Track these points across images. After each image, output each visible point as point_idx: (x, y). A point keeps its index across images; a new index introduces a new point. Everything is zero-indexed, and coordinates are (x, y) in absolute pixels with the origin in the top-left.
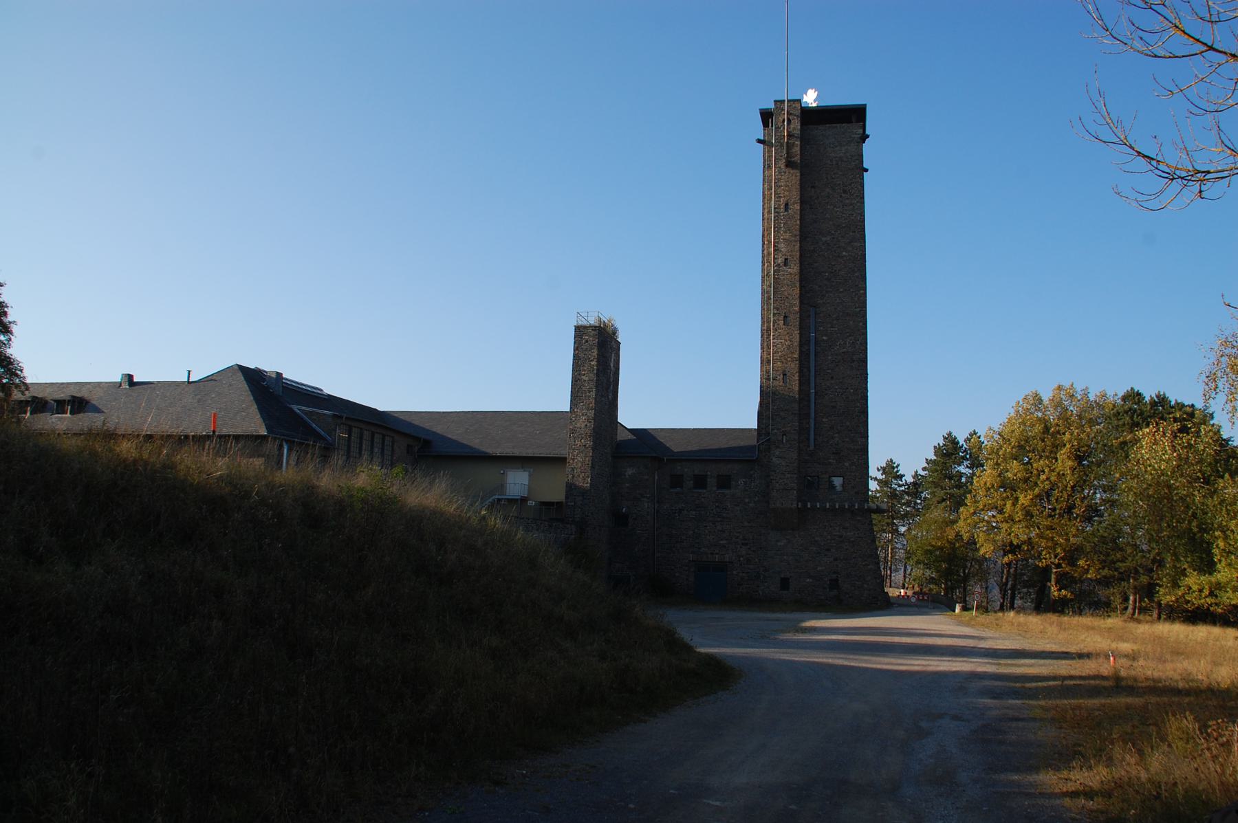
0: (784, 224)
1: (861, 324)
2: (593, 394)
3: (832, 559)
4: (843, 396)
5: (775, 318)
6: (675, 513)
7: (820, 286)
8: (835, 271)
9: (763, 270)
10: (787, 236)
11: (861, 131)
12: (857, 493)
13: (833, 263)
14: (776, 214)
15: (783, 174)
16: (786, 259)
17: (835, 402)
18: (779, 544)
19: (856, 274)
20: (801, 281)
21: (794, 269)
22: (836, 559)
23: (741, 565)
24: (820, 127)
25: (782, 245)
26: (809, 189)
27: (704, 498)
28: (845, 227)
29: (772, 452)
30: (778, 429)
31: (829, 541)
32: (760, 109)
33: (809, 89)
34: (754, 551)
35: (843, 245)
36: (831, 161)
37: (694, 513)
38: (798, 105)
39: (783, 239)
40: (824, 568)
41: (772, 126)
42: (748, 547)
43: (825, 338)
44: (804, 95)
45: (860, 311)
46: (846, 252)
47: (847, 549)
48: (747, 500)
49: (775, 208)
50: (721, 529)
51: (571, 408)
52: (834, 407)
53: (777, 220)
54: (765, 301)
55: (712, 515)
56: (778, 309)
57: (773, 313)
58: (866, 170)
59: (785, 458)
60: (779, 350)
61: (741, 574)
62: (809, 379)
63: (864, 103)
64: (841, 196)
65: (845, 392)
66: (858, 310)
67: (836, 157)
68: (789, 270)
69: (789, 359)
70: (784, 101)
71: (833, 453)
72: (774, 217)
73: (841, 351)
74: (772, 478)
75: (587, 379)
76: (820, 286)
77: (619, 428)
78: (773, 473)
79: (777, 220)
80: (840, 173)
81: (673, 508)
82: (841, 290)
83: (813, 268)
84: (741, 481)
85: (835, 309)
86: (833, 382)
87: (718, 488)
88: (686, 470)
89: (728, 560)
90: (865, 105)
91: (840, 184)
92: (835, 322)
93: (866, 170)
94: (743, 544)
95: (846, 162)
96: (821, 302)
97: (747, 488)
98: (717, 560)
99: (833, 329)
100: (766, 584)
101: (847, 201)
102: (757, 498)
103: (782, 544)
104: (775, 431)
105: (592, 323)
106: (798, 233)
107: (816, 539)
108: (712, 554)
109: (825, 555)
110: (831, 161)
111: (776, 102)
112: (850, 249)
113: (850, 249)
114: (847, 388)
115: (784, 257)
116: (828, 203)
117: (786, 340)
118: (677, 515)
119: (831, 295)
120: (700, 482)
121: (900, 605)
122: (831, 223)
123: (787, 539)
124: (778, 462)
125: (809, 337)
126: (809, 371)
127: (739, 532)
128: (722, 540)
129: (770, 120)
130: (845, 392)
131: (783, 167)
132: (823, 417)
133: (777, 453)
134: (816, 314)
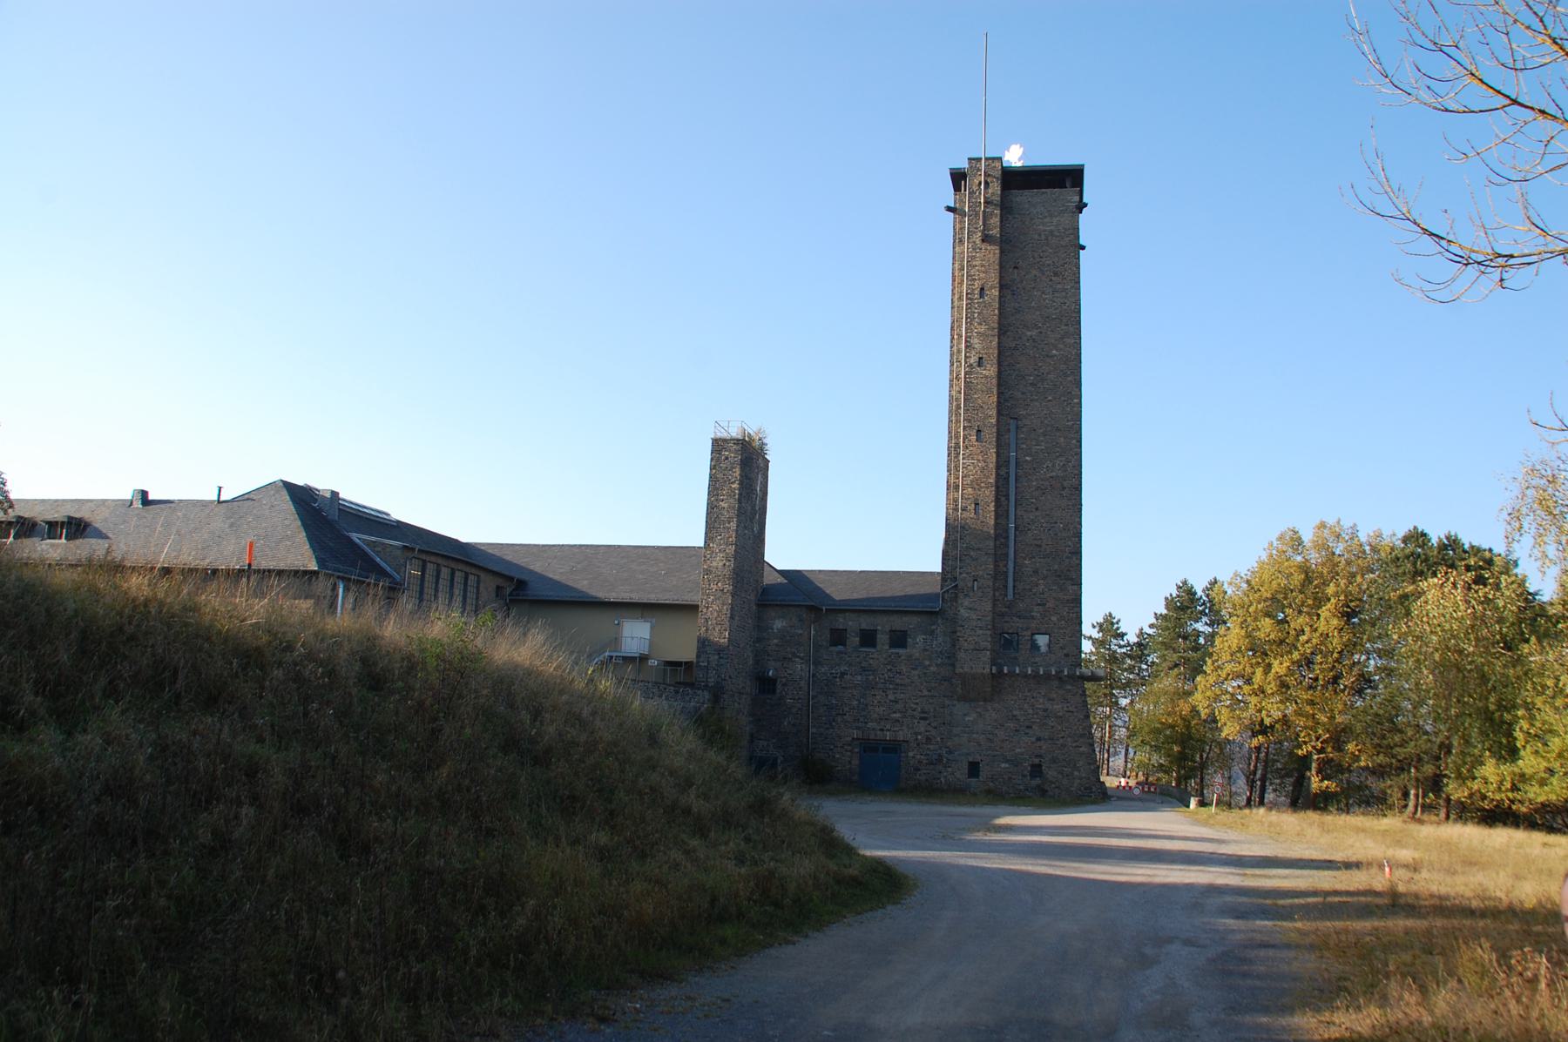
0: (979, 313)
1: (1074, 441)
2: (733, 525)
3: (1034, 739)
4: (1051, 532)
5: (966, 433)
6: (836, 677)
9: (951, 372)
10: (983, 328)
11: (1077, 198)
12: (1067, 655)
13: (1040, 364)
14: (969, 301)
16: (980, 358)
17: (1041, 539)
18: (967, 719)
19: (1069, 379)
20: (999, 385)
21: (990, 371)
22: (1039, 739)
23: (918, 745)
24: (1026, 192)
25: (976, 341)
26: (1011, 270)
27: (873, 658)
29: (960, 602)
30: (967, 573)
32: (951, 169)
33: (1013, 144)
34: (935, 728)
36: (1040, 235)
37: (859, 678)
38: (998, 164)
40: (1023, 750)
41: (965, 190)
42: (928, 722)
43: (1028, 458)
44: (1006, 152)
46: (1057, 350)
47: (1053, 727)
48: (927, 663)
49: (967, 294)
50: (893, 699)
51: (705, 542)
52: (1040, 546)
53: (970, 308)
54: (954, 411)
55: (882, 681)
56: (969, 421)
57: (964, 427)
58: (1083, 248)
59: (976, 610)
61: (918, 757)
62: (1007, 511)
63: (1081, 163)
64: (1051, 280)
67: (1045, 231)
69: (982, 485)
70: (981, 159)
71: (1039, 605)
72: (967, 305)
74: (958, 634)
75: (726, 506)
76: (1023, 393)
77: (767, 569)
78: (961, 629)
79: (970, 308)
80: (1050, 251)
81: (834, 671)
82: (1050, 398)
84: (920, 638)
85: (1042, 422)
86: (1037, 514)
87: (890, 647)
88: (850, 623)
89: (902, 739)
90: (1083, 166)
93: (1083, 248)
94: (922, 718)
96: (1025, 413)
97: (927, 647)
98: (888, 738)
99: (1038, 447)
100: (950, 769)
101: (1059, 286)
102: (940, 660)
104: (964, 575)
105: (734, 435)
106: (996, 326)
107: (1015, 713)
108: (882, 730)
109: (1026, 734)
110: (1040, 235)
111: (969, 159)
112: (1061, 346)
113: (1061, 346)
114: (1056, 523)
116: (1034, 288)
117: (979, 460)
118: (838, 680)
119: (1037, 404)
120: (868, 638)
121: (1119, 798)
122: (1038, 313)
124: (967, 615)
125: (1009, 457)
126: (1008, 499)
127: (917, 704)
128: (895, 712)
129: (963, 183)
131: (978, 241)
133: (966, 603)
134: (1017, 428)
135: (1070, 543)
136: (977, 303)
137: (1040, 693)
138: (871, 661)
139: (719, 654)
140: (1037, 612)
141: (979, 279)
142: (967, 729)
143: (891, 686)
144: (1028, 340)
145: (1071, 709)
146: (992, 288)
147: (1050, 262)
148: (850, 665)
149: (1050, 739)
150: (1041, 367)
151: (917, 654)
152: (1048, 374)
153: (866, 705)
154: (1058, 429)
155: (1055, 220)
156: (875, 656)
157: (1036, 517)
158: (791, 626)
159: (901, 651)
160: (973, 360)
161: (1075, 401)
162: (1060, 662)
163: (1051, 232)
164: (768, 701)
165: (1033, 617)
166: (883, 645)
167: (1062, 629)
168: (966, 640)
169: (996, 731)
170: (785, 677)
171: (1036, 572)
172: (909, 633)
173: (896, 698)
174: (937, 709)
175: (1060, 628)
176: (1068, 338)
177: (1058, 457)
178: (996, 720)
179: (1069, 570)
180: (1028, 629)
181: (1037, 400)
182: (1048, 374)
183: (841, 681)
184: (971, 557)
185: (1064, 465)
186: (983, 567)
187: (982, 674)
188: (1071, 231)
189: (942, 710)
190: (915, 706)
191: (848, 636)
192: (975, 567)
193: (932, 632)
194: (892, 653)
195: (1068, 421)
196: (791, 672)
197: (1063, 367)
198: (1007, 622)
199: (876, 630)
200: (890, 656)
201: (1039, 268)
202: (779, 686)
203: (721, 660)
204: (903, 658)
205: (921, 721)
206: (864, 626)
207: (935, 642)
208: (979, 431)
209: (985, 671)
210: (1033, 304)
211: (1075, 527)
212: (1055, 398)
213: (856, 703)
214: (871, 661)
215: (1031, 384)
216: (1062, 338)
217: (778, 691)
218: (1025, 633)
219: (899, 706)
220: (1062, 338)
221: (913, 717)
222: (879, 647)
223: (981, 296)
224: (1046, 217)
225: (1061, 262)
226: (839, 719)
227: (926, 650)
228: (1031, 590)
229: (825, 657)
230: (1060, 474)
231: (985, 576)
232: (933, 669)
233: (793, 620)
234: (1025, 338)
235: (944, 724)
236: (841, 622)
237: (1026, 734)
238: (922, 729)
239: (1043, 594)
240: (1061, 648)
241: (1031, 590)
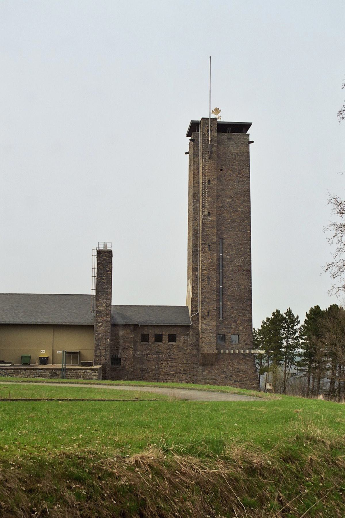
0: (208, 192)
4: (238, 290)
5: (203, 246)
6: (145, 356)
7: (225, 227)
8: (234, 219)
10: (210, 199)
12: (246, 344)
13: (232, 215)
15: (207, 162)
16: (209, 212)
18: (204, 373)
22: (235, 381)
25: (207, 204)
27: (161, 347)
28: (239, 194)
30: (205, 309)
31: (232, 371)
34: (190, 377)
35: (238, 204)
36: (232, 155)
37: (155, 356)
43: (228, 257)
45: (248, 242)
46: (240, 208)
47: (241, 376)
48: (186, 349)
49: (202, 182)
50: (171, 365)
52: (234, 296)
55: (166, 357)
60: (205, 264)
64: (237, 176)
65: (239, 288)
66: (246, 242)
68: (211, 219)
69: (211, 270)
71: (235, 322)
76: (225, 227)
78: (203, 333)
81: (143, 353)
82: (237, 230)
83: (221, 217)
84: (182, 338)
85: (234, 241)
87: (169, 341)
91: (236, 169)
95: (240, 156)
97: (186, 341)
99: (232, 252)
102: (191, 347)
103: (206, 373)
104: (204, 310)
107: (225, 370)
109: (230, 379)
110: (232, 155)
114: (241, 286)
116: (229, 180)
117: (209, 258)
118: (145, 357)
120: (159, 338)
122: (232, 191)
123: (208, 370)
124: (205, 327)
127: (181, 367)
128: (172, 371)
130: (239, 288)
131: (207, 158)
132: (227, 302)
133: (205, 323)
134: (223, 243)
135: (247, 295)
136: (207, 187)
137: (235, 361)
138: (160, 348)
139: (105, 349)
140: (234, 325)
141: (208, 176)
142: (204, 378)
143: (170, 360)
144: (227, 203)
145: (249, 368)
146: (213, 180)
148: (151, 350)
149: (240, 381)
150: (233, 216)
151: (181, 345)
153: (159, 368)
154: (241, 244)
155: (239, 148)
157: (232, 283)
158: (128, 334)
159: (174, 343)
160: (206, 213)
161: (248, 231)
162: (244, 348)
163: (237, 153)
164: (117, 368)
165: (232, 328)
166: (166, 341)
167: (244, 333)
168: (205, 339)
169: (217, 378)
170: (125, 357)
171: (232, 307)
172: (177, 335)
173: (172, 364)
174: (191, 369)
175: (243, 332)
176: (245, 203)
177: (241, 257)
178: (216, 374)
180: (229, 333)
181: (232, 231)
183: (147, 358)
184: (207, 302)
185: (243, 260)
186: (212, 306)
187: (213, 354)
191: (149, 337)
192: (208, 306)
193: (187, 335)
194: (170, 344)
195: (245, 240)
196: (128, 355)
197: (243, 216)
198: (220, 330)
199: (162, 334)
200: (169, 346)
201: (232, 170)
202: (122, 361)
203: (106, 352)
204: (175, 346)
205: (184, 375)
206: (156, 333)
207: (189, 339)
209: (214, 352)
211: (249, 288)
212: (239, 230)
213: (154, 367)
214: (160, 348)
215: (229, 224)
216: (242, 203)
217: (122, 364)
218: (228, 335)
220: (242, 203)
221: (180, 373)
222: (164, 342)
223: (209, 183)
224: (235, 146)
225: (242, 168)
226: (146, 375)
227: (185, 343)
228: (230, 315)
229: (139, 347)
230: (242, 264)
231: (213, 310)
232: (188, 351)
233: (128, 331)
234: (226, 202)
235: (194, 376)
236: (146, 331)
237: (230, 379)
238: (184, 378)
239: (236, 317)
240: (244, 341)
241: (230, 315)
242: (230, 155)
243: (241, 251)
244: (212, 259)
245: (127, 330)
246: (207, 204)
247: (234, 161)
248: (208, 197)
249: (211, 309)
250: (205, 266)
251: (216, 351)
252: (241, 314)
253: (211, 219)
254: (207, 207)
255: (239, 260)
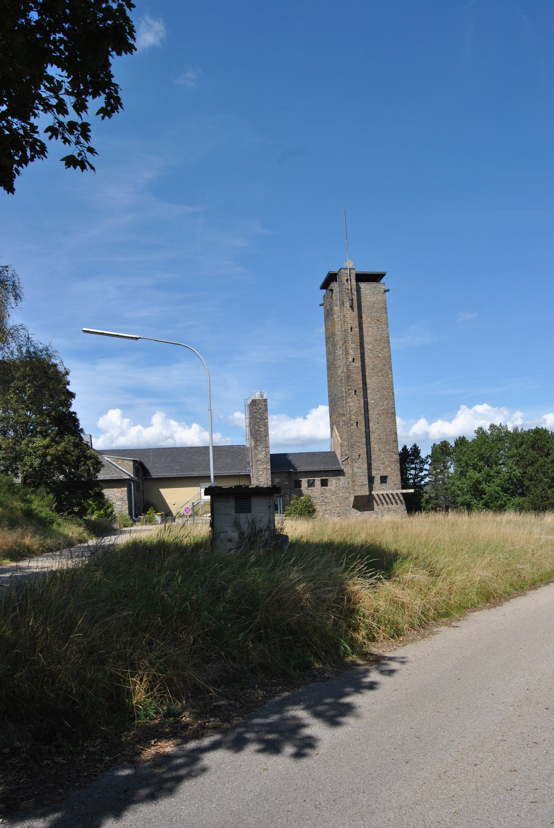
10: (353, 346)
12: (395, 484)
16: (353, 359)
19: (387, 366)
36: (370, 303)
39: (351, 347)
43: (373, 401)
48: (338, 492)
52: (381, 439)
59: (361, 468)
66: (389, 386)
68: (356, 365)
71: (382, 464)
73: (382, 408)
82: (379, 375)
84: (334, 482)
86: (378, 425)
92: (377, 392)
101: (380, 326)
106: (359, 344)
112: (383, 352)
113: (383, 352)
115: (352, 357)
119: (375, 377)
122: (372, 338)
124: (357, 471)
138: (314, 493)
146: (355, 327)
147: (375, 315)
152: (378, 364)
154: (384, 388)
155: (376, 296)
156: (315, 491)
157: (378, 426)
160: (350, 360)
163: (374, 301)
166: (318, 486)
171: (380, 450)
179: (393, 449)
182: (378, 364)
188: (383, 302)
189: (346, 512)
190: (335, 511)
197: (384, 361)
208: (355, 391)
210: (369, 334)
212: (382, 375)
214: (314, 493)
216: (383, 349)
218: (378, 476)
219: (328, 512)
220: (383, 349)
224: (372, 295)
225: (380, 315)
232: (341, 494)
241: (378, 458)
242: (368, 304)
243: (384, 395)
244: (359, 404)
245: (282, 478)
246: (351, 351)
247: (372, 309)
248: (352, 343)
249: (361, 452)
250: (353, 410)
251: (368, 494)
252: (388, 456)
253: (356, 365)
254: (351, 353)
255: (383, 404)
